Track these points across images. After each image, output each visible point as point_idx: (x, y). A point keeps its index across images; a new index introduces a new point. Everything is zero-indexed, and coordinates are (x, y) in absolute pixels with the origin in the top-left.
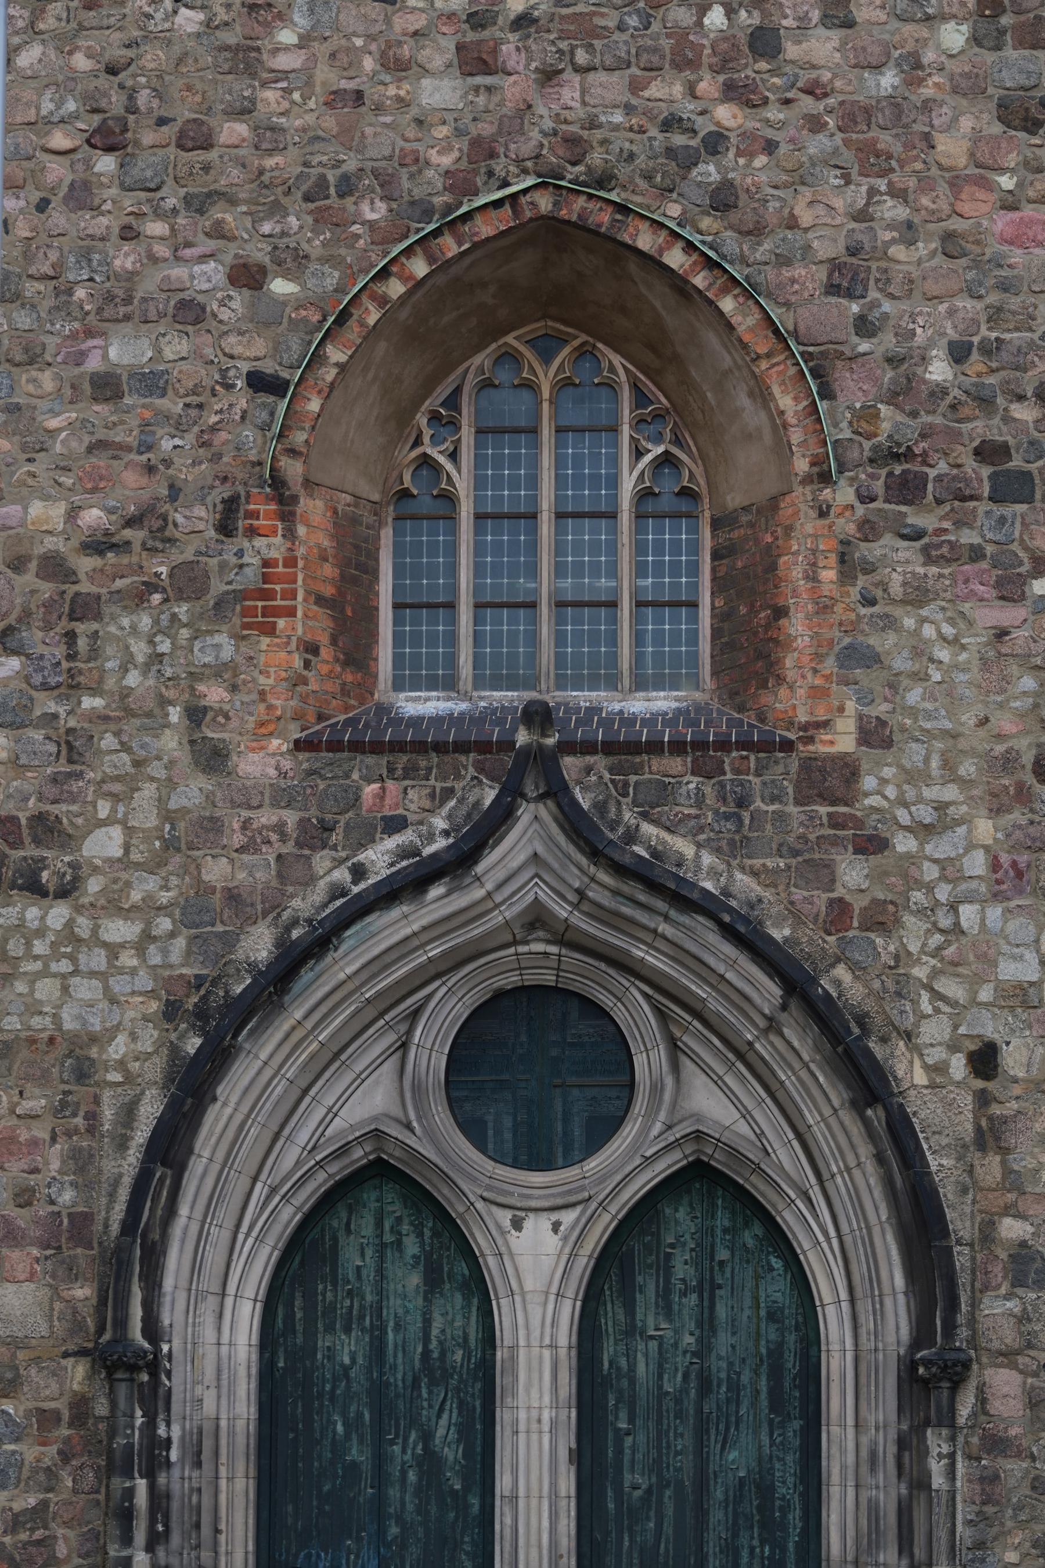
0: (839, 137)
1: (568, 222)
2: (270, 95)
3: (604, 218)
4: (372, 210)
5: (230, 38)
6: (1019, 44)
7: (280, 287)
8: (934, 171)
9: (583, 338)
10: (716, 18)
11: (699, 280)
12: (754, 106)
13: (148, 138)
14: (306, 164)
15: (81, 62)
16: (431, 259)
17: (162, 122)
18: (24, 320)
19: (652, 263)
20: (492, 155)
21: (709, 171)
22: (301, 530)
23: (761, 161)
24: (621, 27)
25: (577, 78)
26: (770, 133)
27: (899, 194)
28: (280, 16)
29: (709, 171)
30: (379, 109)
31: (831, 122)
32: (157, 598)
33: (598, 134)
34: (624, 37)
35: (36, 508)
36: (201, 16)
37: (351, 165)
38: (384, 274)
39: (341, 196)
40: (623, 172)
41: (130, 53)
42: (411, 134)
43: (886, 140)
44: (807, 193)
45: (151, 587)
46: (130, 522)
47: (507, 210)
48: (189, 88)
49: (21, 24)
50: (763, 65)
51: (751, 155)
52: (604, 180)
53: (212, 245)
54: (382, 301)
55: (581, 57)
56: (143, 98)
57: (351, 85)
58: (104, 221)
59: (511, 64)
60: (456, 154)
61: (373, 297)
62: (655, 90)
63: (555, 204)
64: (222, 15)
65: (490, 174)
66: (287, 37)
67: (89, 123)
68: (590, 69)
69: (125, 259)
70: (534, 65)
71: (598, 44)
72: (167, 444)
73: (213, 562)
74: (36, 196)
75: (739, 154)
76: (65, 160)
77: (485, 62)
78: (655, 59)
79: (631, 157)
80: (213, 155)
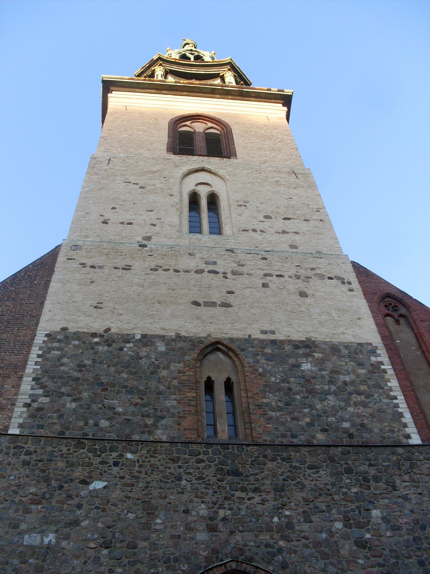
0: (314, 550)
1: (241, 571)
2: (154, 535)
4: (184, 566)
5: (143, 520)
6: (356, 527)
8: (341, 559)
10: (276, 519)
12: (290, 541)
14: (164, 554)
15: (100, 525)
17: (122, 541)
20: (218, 553)
23: (293, 556)
26: (294, 548)
27: (332, 564)
28: (157, 516)
30: (185, 539)
31: (311, 545)
33: (247, 548)
34: (252, 524)
36: (134, 515)
37: (177, 554)
39: (174, 562)
41: (114, 523)
42: (194, 547)
43: (326, 550)
44: (308, 564)
48: (130, 533)
49: (84, 515)
50: (290, 531)
51: (290, 554)
52: (251, 560)
55: (241, 528)
56: (117, 535)
57: (177, 534)
58: (103, 568)
59: (222, 530)
60: (207, 552)
62: (261, 537)
63: (237, 566)
64: (141, 515)
65: (217, 558)
66: (158, 521)
67: (101, 541)
68: (242, 532)
70: (228, 530)
71: (245, 525)
75: (287, 553)
76: (93, 551)
77: (214, 529)
78: (261, 529)
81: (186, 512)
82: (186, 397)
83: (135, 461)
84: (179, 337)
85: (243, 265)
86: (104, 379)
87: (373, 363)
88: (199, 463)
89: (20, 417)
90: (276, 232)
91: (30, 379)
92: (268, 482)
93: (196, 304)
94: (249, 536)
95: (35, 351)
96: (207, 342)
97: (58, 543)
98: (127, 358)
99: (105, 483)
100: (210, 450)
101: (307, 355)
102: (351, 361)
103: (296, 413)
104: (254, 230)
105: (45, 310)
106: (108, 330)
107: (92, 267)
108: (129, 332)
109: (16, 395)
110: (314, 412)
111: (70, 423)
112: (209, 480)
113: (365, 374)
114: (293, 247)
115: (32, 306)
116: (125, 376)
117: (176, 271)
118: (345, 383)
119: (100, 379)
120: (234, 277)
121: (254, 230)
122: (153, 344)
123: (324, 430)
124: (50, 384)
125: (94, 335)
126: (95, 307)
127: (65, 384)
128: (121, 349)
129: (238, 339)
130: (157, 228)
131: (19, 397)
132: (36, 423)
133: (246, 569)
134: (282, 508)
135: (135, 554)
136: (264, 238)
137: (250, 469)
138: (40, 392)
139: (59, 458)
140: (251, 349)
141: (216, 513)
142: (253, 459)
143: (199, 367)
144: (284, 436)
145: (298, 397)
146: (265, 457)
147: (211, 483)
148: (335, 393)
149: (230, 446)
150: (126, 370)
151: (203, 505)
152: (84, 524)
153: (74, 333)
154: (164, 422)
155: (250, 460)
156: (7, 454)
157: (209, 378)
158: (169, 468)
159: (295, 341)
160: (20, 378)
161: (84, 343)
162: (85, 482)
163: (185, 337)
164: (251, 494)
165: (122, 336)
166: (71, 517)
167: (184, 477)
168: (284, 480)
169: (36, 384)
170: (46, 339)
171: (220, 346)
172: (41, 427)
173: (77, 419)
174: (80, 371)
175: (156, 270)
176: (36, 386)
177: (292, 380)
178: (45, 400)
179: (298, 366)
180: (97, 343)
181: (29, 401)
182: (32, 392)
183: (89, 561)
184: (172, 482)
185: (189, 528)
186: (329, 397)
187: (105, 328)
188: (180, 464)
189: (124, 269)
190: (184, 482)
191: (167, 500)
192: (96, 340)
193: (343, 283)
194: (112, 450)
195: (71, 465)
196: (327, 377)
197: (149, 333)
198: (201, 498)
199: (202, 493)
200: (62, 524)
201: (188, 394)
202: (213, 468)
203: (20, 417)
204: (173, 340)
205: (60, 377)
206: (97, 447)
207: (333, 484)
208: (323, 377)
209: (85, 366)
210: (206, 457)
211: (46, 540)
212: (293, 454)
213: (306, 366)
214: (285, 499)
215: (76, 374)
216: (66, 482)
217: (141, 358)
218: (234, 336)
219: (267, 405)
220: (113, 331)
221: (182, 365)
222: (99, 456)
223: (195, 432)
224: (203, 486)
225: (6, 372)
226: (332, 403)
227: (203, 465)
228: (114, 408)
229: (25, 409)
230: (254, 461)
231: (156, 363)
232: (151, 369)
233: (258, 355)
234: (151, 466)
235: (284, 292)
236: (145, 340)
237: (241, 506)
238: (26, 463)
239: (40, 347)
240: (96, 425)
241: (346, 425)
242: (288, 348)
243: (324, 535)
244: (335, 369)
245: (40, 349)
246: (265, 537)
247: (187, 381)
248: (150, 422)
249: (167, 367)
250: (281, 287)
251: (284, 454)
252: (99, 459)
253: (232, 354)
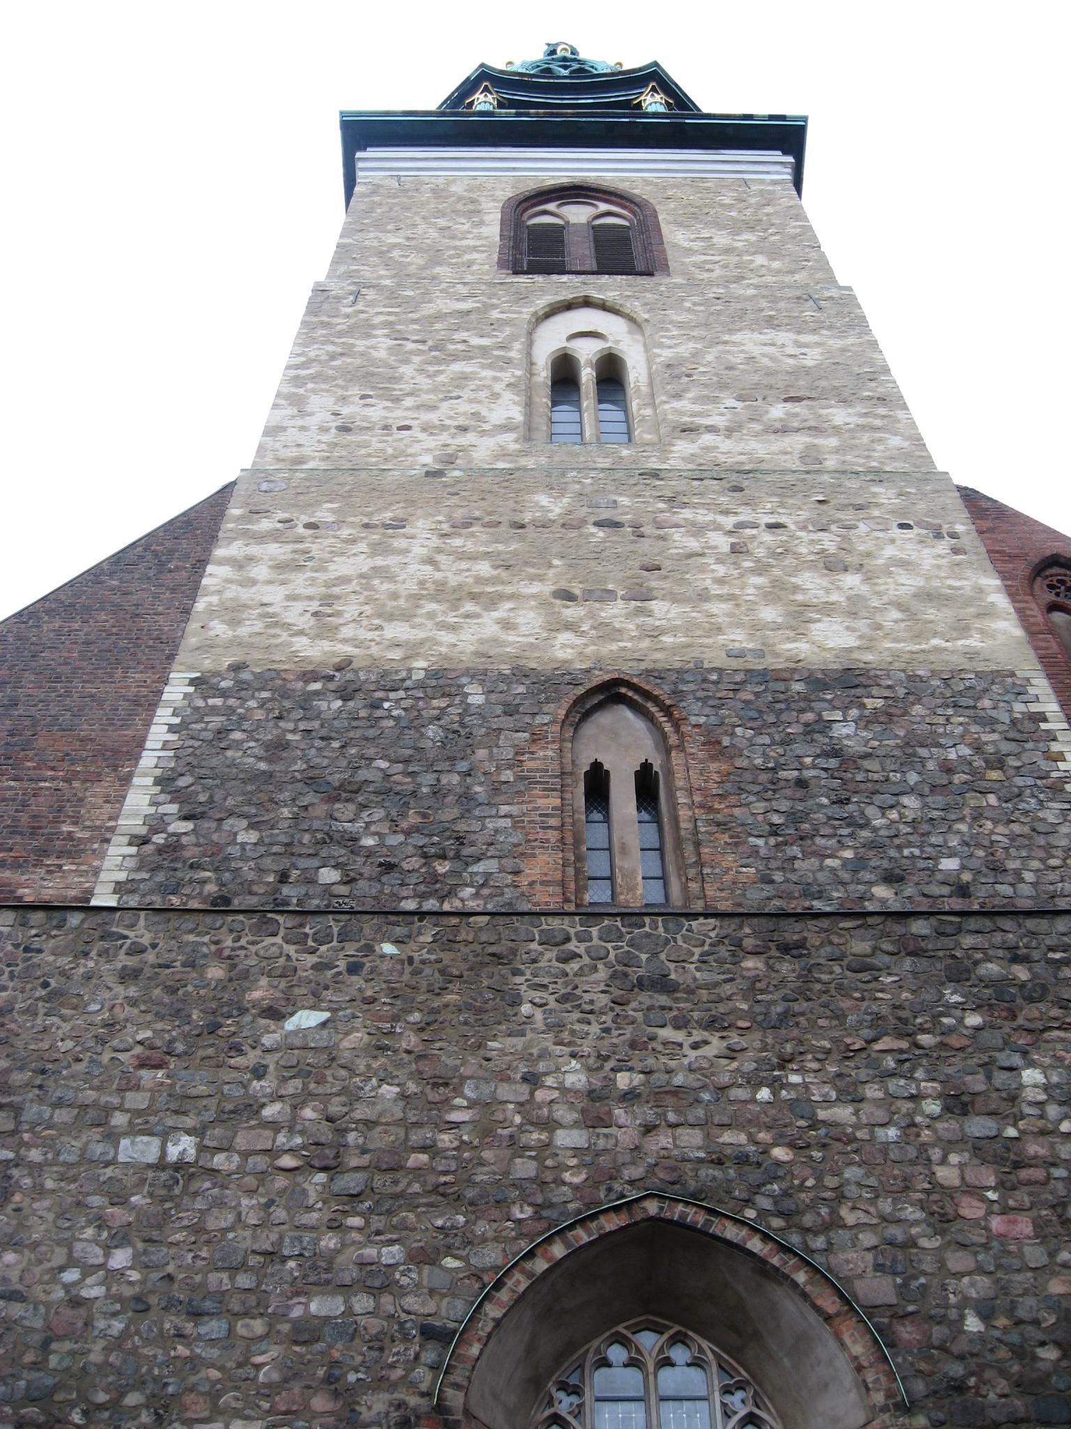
4: (522, 1212)
9: (677, 1328)
11: (775, 1261)
12: (801, 1148)
15: (308, 1113)
16: (567, 1244)
17: (364, 1151)
25: (670, 1131)
36: (397, 1089)
38: (530, 1255)
49: (269, 1090)
54: (529, 1275)
55: (672, 1117)
58: (315, 1215)
59: (622, 1121)
61: (523, 1271)
63: (661, 1208)
68: (677, 1125)
69: (329, 1242)
70: (638, 1122)
77: (602, 1119)
82: (536, 809)
83: (402, 962)
88: (565, 960)
89: (120, 868)
91: (149, 781)
99: (327, 1015)
100: (595, 931)
112: (592, 1002)
125: (311, 676)
131: (120, 822)
133: (684, 1215)
137: (698, 975)
138: (173, 808)
142: (706, 948)
143: (573, 740)
149: (647, 920)
151: (574, 1062)
155: (697, 951)
157: (597, 766)
160: (126, 780)
162: (275, 1014)
164: (698, 1035)
169: (162, 792)
171: (623, 690)
176: (162, 798)
181: (143, 831)
186: (905, 800)
190: (526, 1009)
192: (316, 686)
198: (569, 1044)
199: (573, 1032)
202: (602, 974)
206: (307, 930)
211: (173, 1152)
223: (558, 890)
224: (576, 1015)
227: (574, 966)
228: (355, 840)
229: (133, 850)
238: (128, 976)
239: (175, 709)
247: (538, 770)
252: (312, 959)
253: (654, 709)
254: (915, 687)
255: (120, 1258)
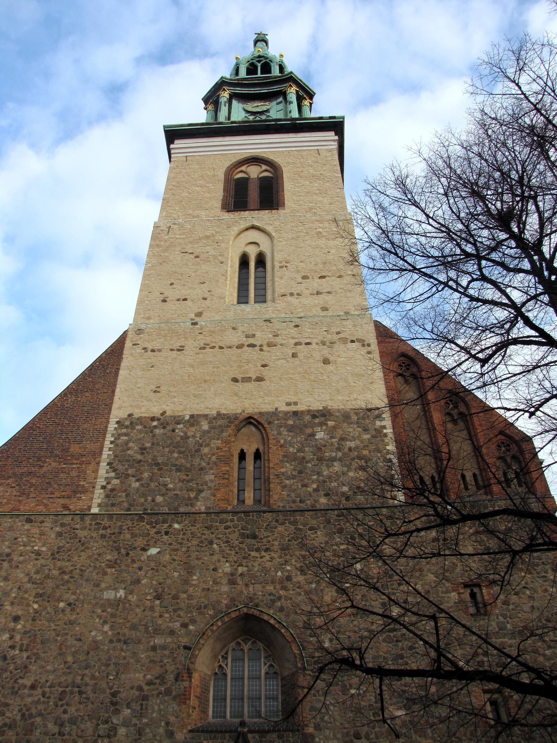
3: (257, 613)
7: (191, 627)
10: (279, 574)
11: (277, 626)
13: (166, 597)
16: (222, 622)
17: (169, 594)
18: (138, 634)
19: (267, 622)
20: (235, 601)
21: (278, 604)
22: (193, 680)
24: (261, 576)
25: (252, 586)
29: (278, 604)
30: (212, 591)
32: (161, 696)
35: (137, 675)
37: (206, 603)
38: (212, 625)
40: (261, 604)
45: (160, 693)
46: (156, 678)
47: (238, 612)
52: (257, 605)
53: (177, 619)
54: (212, 631)
55: (253, 581)
56: (166, 589)
64: (182, 574)
66: (195, 578)
69: (160, 621)
72: (166, 661)
73: (173, 687)
74: (143, 609)
76: (149, 602)
79: (263, 601)
80: (179, 601)
81: (215, 570)
84: (219, 415)
85: (277, 336)
86: (160, 460)
87: (377, 427)
88: (227, 529)
89: (99, 498)
90: (311, 294)
92: (276, 543)
93: (235, 380)
94: (258, 587)
95: (109, 438)
96: (241, 418)
97: (126, 597)
98: (178, 439)
100: (235, 518)
101: (321, 424)
102: (358, 427)
103: (306, 480)
104: (292, 294)
105: (116, 398)
106: (163, 413)
107: (153, 351)
108: (180, 414)
109: (95, 478)
110: (321, 478)
111: (134, 500)
113: (369, 439)
114: (324, 309)
115: (105, 395)
116: (176, 455)
117: (221, 348)
118: (350, 449)
119: (157, 460)
120: (269, 349)
121: (292, 294)
122: (198, 423)
123: (327, 495)
124: (120, 467)
125: (153, 419)
126: (155, 392)
127: (131, 467)
128: (173, 431)
129: (267, 413)
130: (208, 302)
132: (110, 502)
134: (285, 564)
135: (177, 603)
136: (300, 302)
138: (113, 474)
139: (126, 531)
140: (276, 422)
141: (236, 569)
144: (294, 502)
145: (310, 465)
146: (277, 521)
147: (234, 545)
148: (340, 460)
150: (176, 450)
152: (144, 581)
153: (138, 419)
154: (203, 495)
155: (265, 525)
156: (90, 529)
158: (205, 534)
159: (314, 411)
160: (98, 463)
161: (145, 427)
162: (144, 550)
163: (224, 414)
164: (263, 553)
165: (175, 417)
166: (135, 577)
167: (215, 541)
168: (289, 541)
170: (116, 426)
171: (252, 421)
172: (113, 505)
173: (140, 497)
174: (142, 454)
175: (204, 348)
177: (307, 449)
178: (116, 482)
179: (313, 435)
180: (155, 427)
181: (104, 484)
182: (107, 475)
183: (147, 610)
184: (206, 546)
185: (215, 582)
186: (335, 464)
187: (161, 412)
188: (212, 531)
189: (178, 350)
190: (215, 546)
191: (202, 561)
192: (155, 423)
193: (363, 345)
194: (164, 521)
195: (134, 535)
196: (336, 445)
197: (196, 413)
199: (227, 554)
200: (129, 583)
201: (223, 469)
202: (237, 533)
203: (99, 498)
204: (215, 418)
205: (128, 461)
207: (327, 543)
208: (332, 444)
209: (145, 449)
210: (232, 524)
211: (118, 595)
212: (298, 518)
213: (320, 435)
214: (288, 557)
215: (139, 457)
216: (131, 550)
217: (188, 438)
218: (263, 411)
219: (283, 474)
220: (168, 414)
221: (220, 441)
222: (154, 527)
224: (228, 548)
225: (88, 459)
226: (336, 469)
227: (229, 530)
228: (167, 485)
229: (102, 491)
230: (268, 525)
231: (200, 441)
232: (197, 447)
233: (281, 427)
234: (192, 533)
235: (311, 360)
236: (192, 420)
237: (254, 564)
238: (103, 536)
240: (153, 500)
241: (345, 489)
242: (308, 418)
243: (314, 586)
244: (344, 436)
245: (112, 436)
246: (270, 588)
247: (223, 456)
248: (192, 495)
249: (208, 445)
250: (309, 355)
251: (292, 518)
252: (155, 530)
253: (261, 428)
254: (346, 416)
255: (106, 628)
